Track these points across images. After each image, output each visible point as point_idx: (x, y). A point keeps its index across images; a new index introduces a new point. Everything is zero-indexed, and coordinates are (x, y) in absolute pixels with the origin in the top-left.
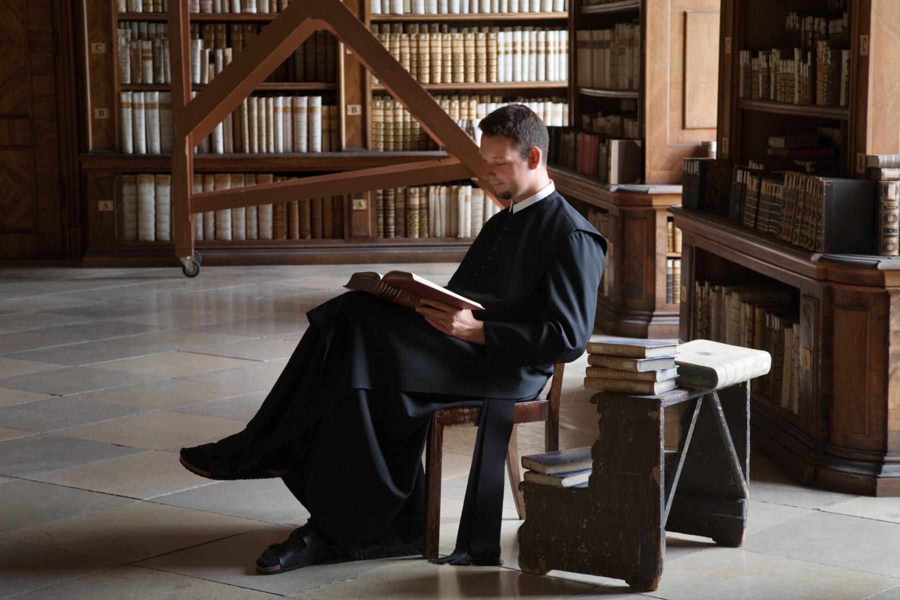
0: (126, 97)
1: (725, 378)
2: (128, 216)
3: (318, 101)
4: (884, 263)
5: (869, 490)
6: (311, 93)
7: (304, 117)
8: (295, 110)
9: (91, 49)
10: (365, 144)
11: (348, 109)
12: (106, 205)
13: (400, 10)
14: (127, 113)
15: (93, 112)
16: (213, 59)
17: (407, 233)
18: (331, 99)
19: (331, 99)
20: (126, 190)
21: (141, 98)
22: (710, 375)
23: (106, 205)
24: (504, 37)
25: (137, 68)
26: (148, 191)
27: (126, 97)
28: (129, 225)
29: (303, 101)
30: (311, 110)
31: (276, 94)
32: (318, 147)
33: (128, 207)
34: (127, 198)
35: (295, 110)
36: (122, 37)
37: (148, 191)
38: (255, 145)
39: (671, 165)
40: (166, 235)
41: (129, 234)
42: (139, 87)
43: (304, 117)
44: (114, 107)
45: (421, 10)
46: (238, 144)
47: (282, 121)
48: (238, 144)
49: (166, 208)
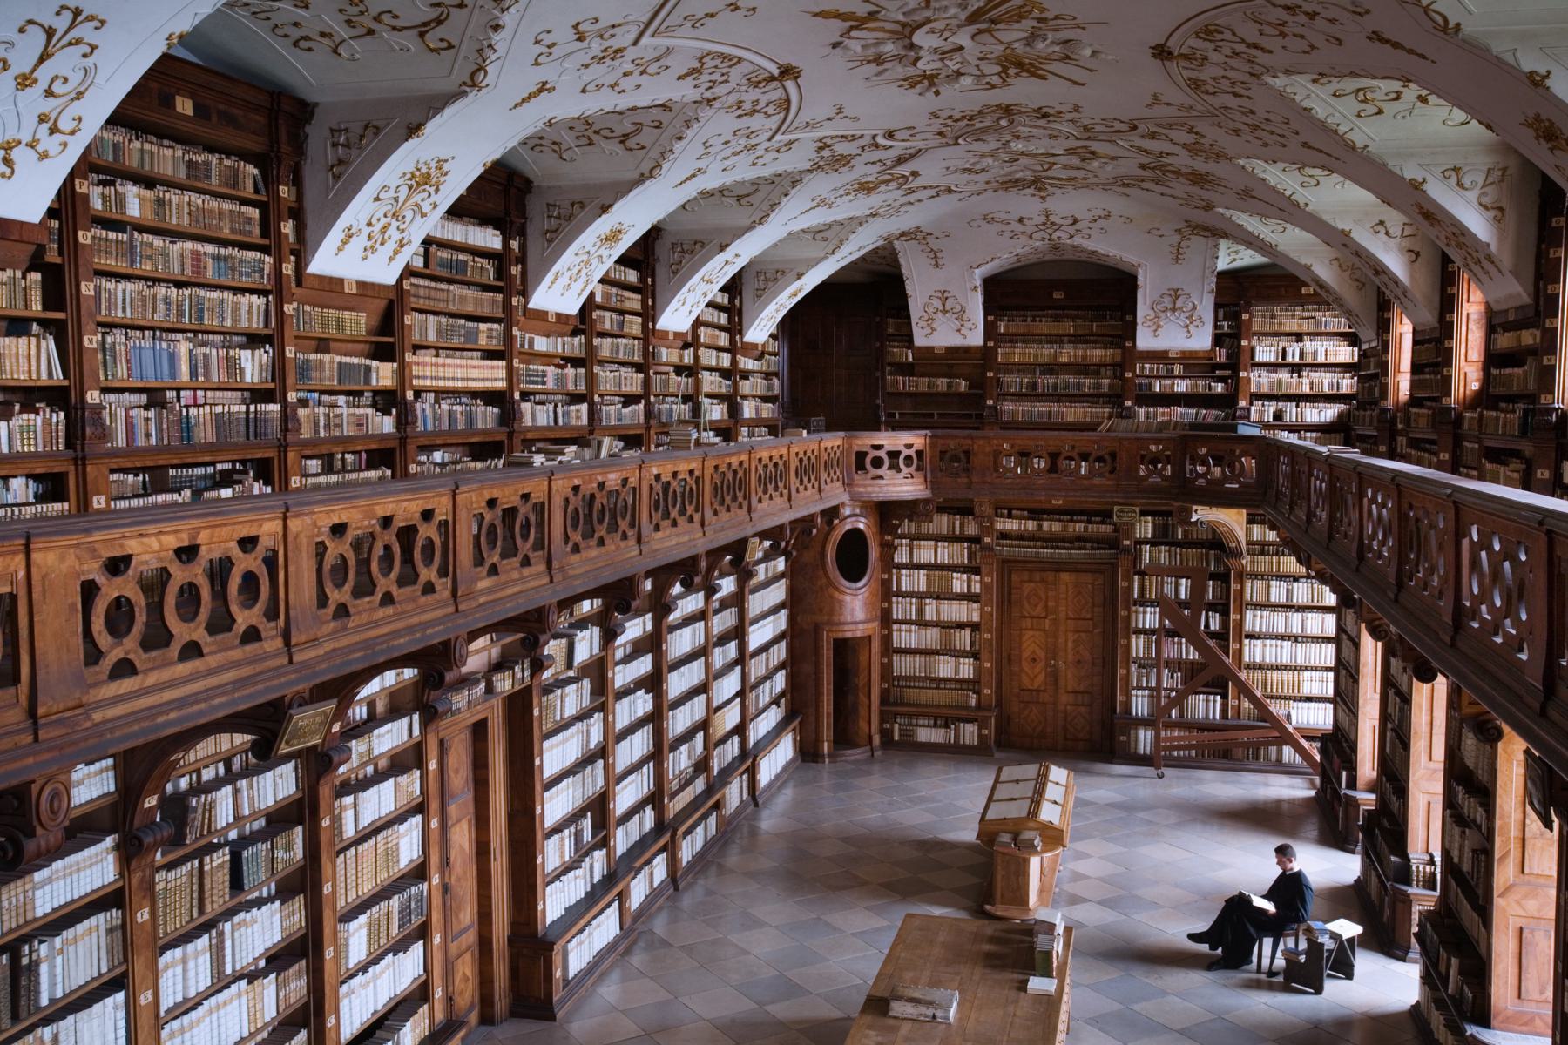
0: (1134, 692)
1: (1345, 936)
2: (1132, 743)
3: (1218, 697)
4: (1410, 890)
5: (1404, 960)
6: (1216, 694)
7: (1211, 704)
8: (1207, 701)
9: (1120, 672)
10: (1239, 718)
11: (1232, 702)
12: (1123, 738)
13: (1257, 660)
14: (1134, 699)
15: (1119, 698)
16: (1172, 677)
17: (1257, 758)
18: (1224, 697)
19: (1224, 697)
20: (1132, 732)
21: (1140, 692)
22: (1340, 936)
23: (1123, 738)
24: (1307, 674)
25: (1139, 680)
26: (1141, 733)
27: (1134, 692)
28: (1132, 746)
29: (1212, 697)
30: (1215, 701)
31: (1200, 693)
32: (1217, 717)
33: (1132, 739)
34: (1132, 735)
35: (1207, 701)
36: (1134, 667)
37: (1141, 733)
38: (1189, 715)
39: (1368, 784)
40: (1148, 752)
41: (1132, 750)
42: (1139, 688)
43: (1211, 704)
44: (1129, 696)
45: (1268, 660)
46: (1181, 715)
47: (1202, 705)
48: (1181, 715)
49: (1149, 741)
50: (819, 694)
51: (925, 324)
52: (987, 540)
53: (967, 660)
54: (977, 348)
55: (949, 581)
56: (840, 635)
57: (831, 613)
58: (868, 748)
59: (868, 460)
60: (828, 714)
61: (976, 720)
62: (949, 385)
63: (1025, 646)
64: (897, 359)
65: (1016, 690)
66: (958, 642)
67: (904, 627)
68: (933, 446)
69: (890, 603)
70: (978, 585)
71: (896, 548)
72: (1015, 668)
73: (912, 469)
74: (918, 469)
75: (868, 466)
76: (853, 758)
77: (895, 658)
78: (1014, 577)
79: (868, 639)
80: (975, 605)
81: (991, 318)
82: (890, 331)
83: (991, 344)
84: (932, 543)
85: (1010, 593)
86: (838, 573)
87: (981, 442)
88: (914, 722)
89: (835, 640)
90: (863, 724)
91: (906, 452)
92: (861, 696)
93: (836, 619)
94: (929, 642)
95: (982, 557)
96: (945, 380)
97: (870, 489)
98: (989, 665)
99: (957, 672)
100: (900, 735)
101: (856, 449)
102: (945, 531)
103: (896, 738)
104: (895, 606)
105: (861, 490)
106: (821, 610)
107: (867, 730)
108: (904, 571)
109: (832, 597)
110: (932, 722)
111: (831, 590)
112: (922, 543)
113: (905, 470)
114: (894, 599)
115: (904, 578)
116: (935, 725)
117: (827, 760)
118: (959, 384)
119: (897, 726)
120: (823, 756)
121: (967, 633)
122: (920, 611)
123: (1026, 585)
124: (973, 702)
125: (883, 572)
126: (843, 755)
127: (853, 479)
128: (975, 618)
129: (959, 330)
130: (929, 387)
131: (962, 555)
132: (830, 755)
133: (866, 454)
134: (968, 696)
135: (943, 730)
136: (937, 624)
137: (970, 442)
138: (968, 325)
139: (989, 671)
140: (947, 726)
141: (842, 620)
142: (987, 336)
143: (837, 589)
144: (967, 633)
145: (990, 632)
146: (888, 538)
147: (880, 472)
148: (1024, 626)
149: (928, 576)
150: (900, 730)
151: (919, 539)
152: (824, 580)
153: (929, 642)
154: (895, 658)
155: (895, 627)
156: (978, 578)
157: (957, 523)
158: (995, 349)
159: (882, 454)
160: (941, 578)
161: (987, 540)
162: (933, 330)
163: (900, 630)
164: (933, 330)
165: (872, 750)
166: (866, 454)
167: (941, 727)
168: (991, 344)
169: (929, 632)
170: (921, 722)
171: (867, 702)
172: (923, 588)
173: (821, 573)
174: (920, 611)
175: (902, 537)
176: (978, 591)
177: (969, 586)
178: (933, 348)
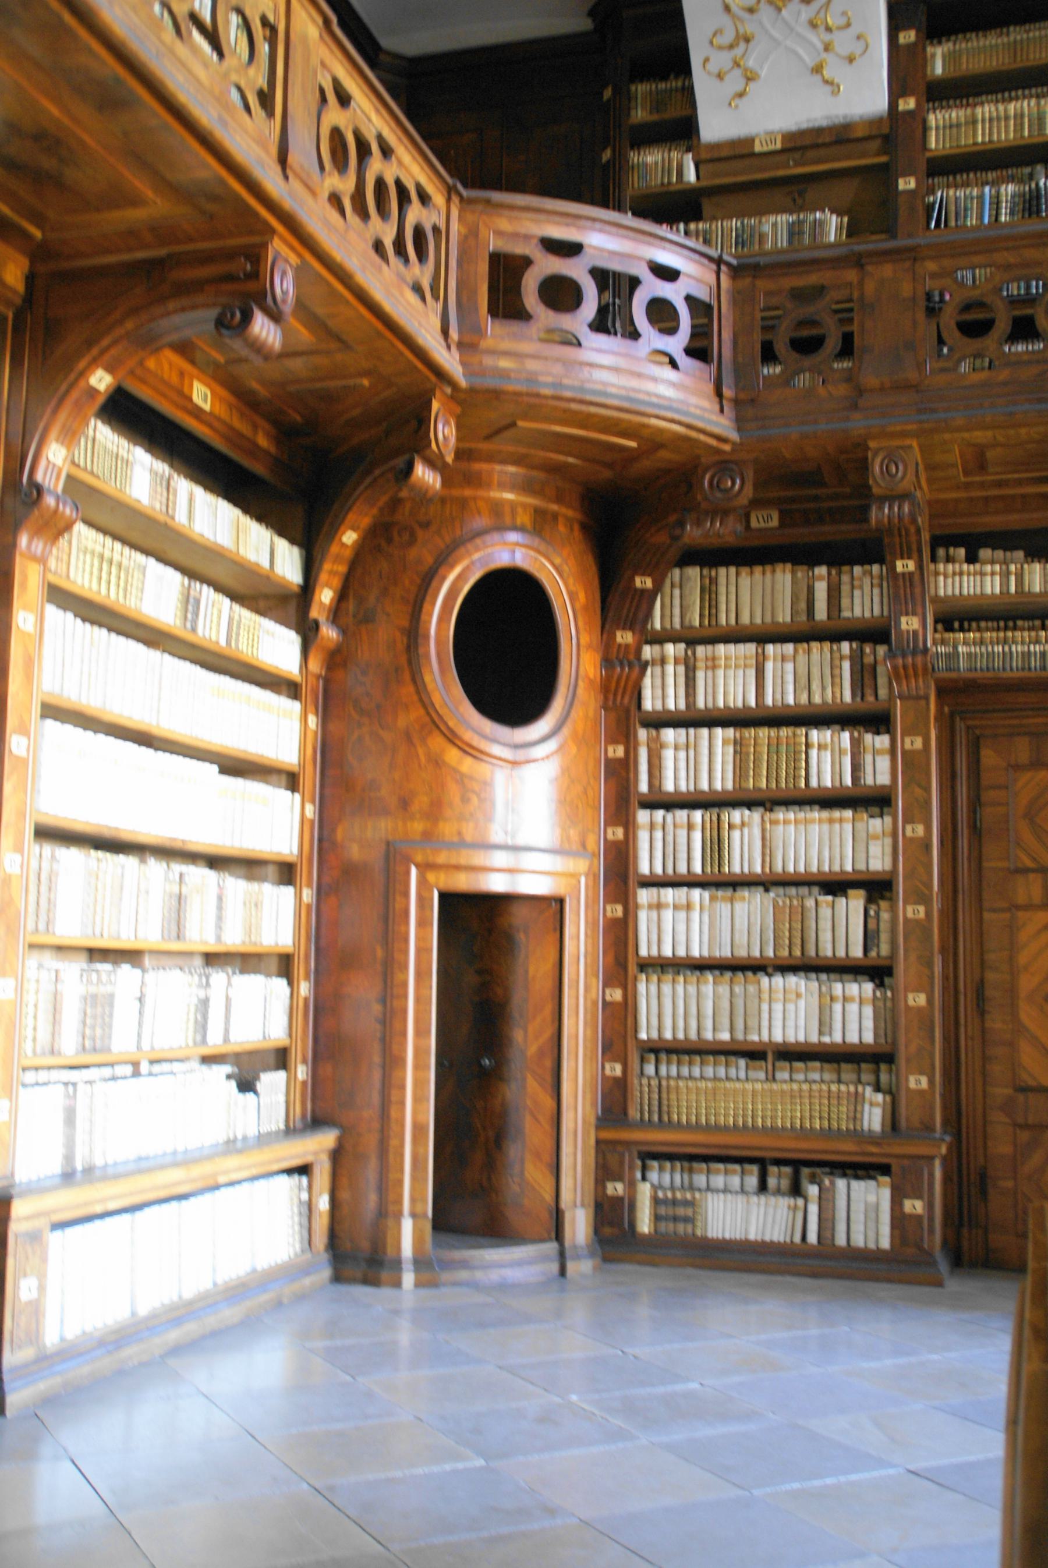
50: (392, 1062)
51: (721, 60)
52: (909, 623)
53: (853, 988)
54: (875, 122)
55: (798, 756)
56: (463, 883)
57: (435, 811)
58: (552, 1247)
59: (530, 284)
60: (419, 1130)
61: (885, 1169)
62: (794, 232)
63: (1022, 958)
64: (655, 181)
65: (1001, 1092)
66: (826, 937)
67: (669, 895)
68: (740, 299)
69: (629, 825)
70: (884, 764)
71: (644, 666)
72: (996, 1022)
73: (676, 344)
74: (698, 351)
75: (531, 299)
76: (494, 1276)
77: (645, 988)
78: (989, 757)
79: (556, 905)
80: (876, 825)
81: (909, 36)
82: (640, 114)
83: (908, 104)
84: (751, 648)
85: (976, 803)
86: (458, 690)
87: (887, 270)
88: (700, 1180)
89: (446, 898)
90: (536, 1174)
91: (652, 287)
92: (532, 1084)
93: (447, 829)
94: (742, 939)
95: (895, 674)
96: (783, 219)
97: (532, 365)
98: (921, 999)
99: (824, 1024)
100: (657, 1218)
101: (494, 244)
102: (784, 616)
103: (645, 1225)
104: (643, 836)
105: (504, 363)
106: (405, 804)
107: (548, 1196)
108: (669, 735)
109: (437, 762)
110: (752, 1181)
111: (437, 742)
112: (721, 649)
113: (651, 338)
114: (643, 816)
115: (668, 755)
116: (763, 1187)
117: (408, 1278)
118: (819, 226)
119: (644, 1191)
120: (397, 1264)
121: (855, 903)
122: (716, 847)
123: (1025, 777)
124: (873, 1118)
125: (612, 740)
126: (465, 1265)
127: (479, 331)
128: (878, 861)
129: (818, 69)
130: (740, 242)
131: (836, 677)
132: (420, 1263)
133: (527, 262)
134: (857, 1099)
135: (784, 1203)
136: (766, 883)
137: (851, 275)
138: (843, 43)
139: (924, 1017)
140: (796, 1190)
141: (469, 833)
142: (898, 87)
143: (452, 738)
144: (855, 903)
145: (924, 899)
146: (625, 637)
147: (568, 322)
148: (1021, 899)
149: (739, 745)
150: (656, 1201)
151: (713, 641)
152: (417, 713)
153: (742, 939)
154: (645, 988)
155: (644, 896)
156: (882, 741)
157: (821, 589)
158: (917, 122)
159: (576, 270)
160: (774, 747)
161: (909, 623)
162: (750, 77)
163: (659, 906)
164: (750, 77)
165: (562, 1255)
166: (527, 262)
167: (778, 1192)
168: (908, 104)
169: (741, 908)
170: (718, 1181)
171: (549, 1103)
172: (723, 780)
173: (408, 690)
174: (716, 847)
175: (659, 639)
176: (884, 778)
177: (856, 768)
178: (750, 141)
